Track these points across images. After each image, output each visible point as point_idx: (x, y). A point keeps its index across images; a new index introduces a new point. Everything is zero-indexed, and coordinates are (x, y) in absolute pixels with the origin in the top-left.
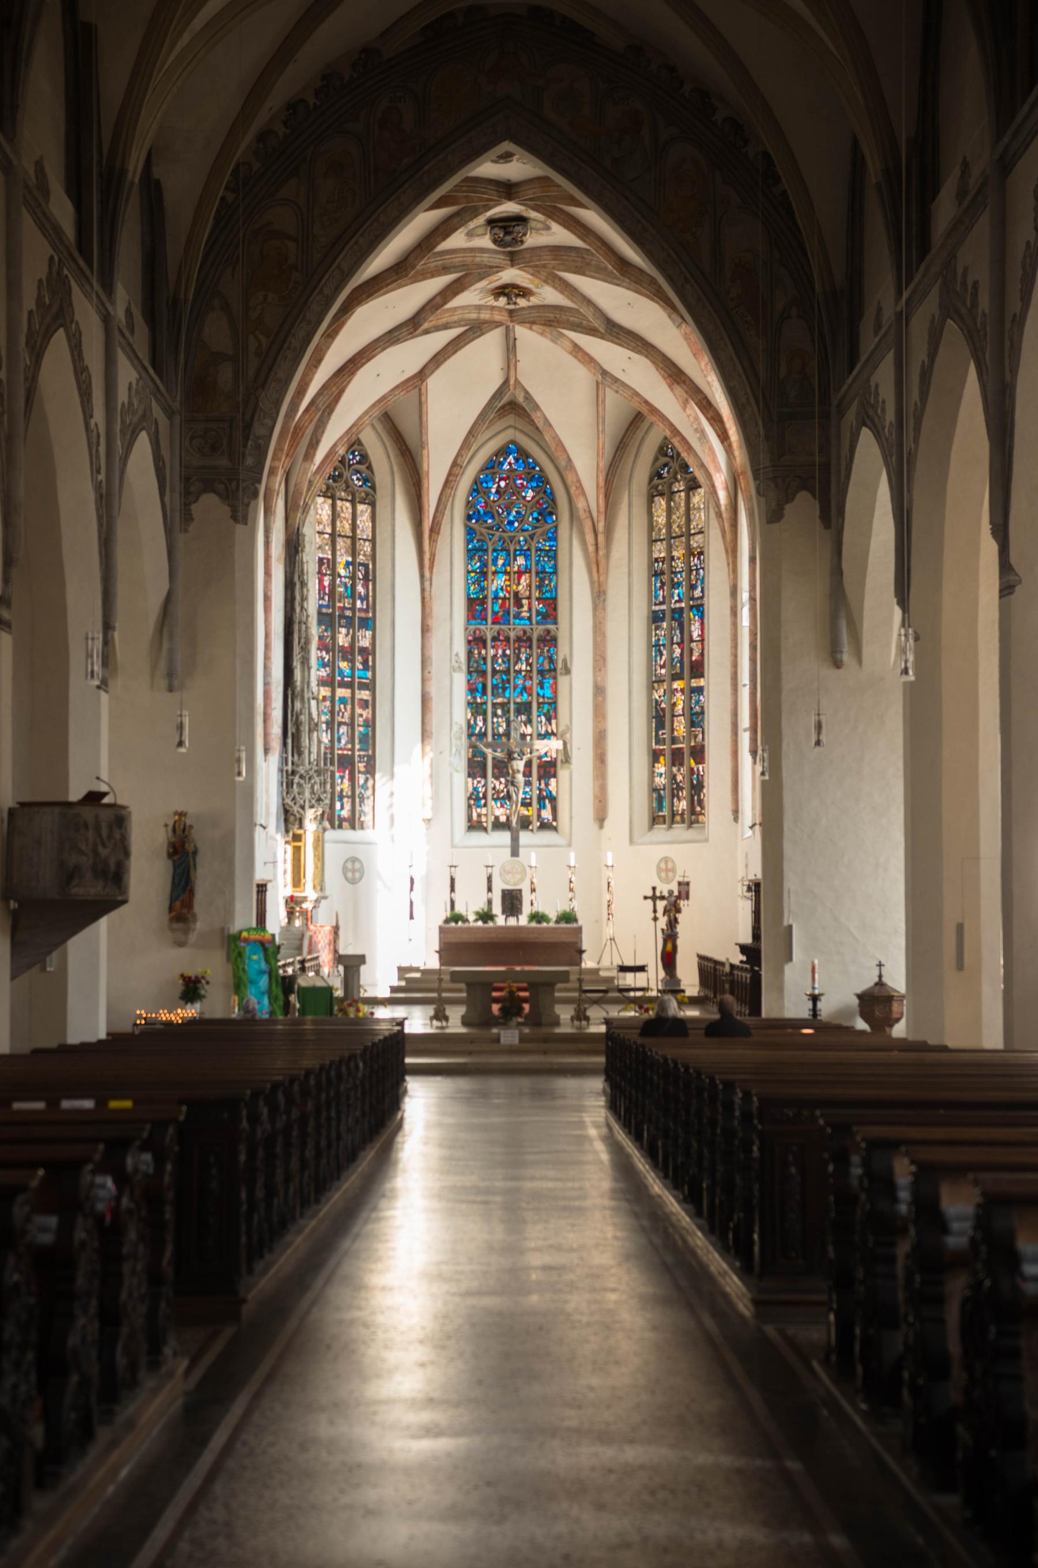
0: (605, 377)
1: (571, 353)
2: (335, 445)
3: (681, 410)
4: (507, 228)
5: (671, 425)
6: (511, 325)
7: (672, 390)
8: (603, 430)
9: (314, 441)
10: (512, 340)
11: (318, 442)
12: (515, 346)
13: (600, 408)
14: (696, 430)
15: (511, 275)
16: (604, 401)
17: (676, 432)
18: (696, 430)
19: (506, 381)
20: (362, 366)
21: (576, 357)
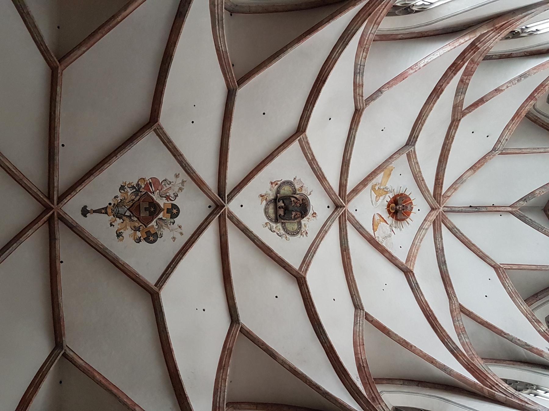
0: (499, 149)
1: (475, 171)
2: (539, 331)
3: (502, 93)
4: (288, 208)
5: (527, 100)
6: (441, 209)
7: (487, 101)
8: (545, 148)
9: (527, 347)
10: (470, 209)
11: (527, 345)
12: (476, 207)
13: (524, 151)
14: (518, 81)
15: (367, 208)
16: (520, 149)
17: (531, 97)
18: (518, 81)
19: (511, 213)
20: (431, 311)
21: (479, 168)
